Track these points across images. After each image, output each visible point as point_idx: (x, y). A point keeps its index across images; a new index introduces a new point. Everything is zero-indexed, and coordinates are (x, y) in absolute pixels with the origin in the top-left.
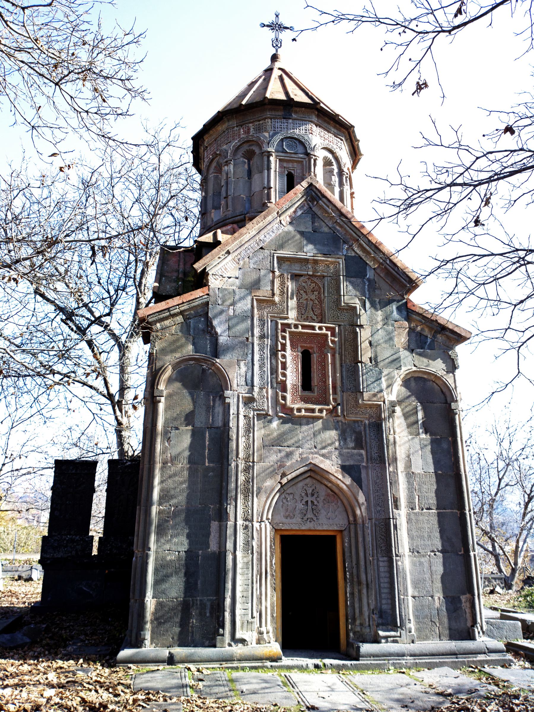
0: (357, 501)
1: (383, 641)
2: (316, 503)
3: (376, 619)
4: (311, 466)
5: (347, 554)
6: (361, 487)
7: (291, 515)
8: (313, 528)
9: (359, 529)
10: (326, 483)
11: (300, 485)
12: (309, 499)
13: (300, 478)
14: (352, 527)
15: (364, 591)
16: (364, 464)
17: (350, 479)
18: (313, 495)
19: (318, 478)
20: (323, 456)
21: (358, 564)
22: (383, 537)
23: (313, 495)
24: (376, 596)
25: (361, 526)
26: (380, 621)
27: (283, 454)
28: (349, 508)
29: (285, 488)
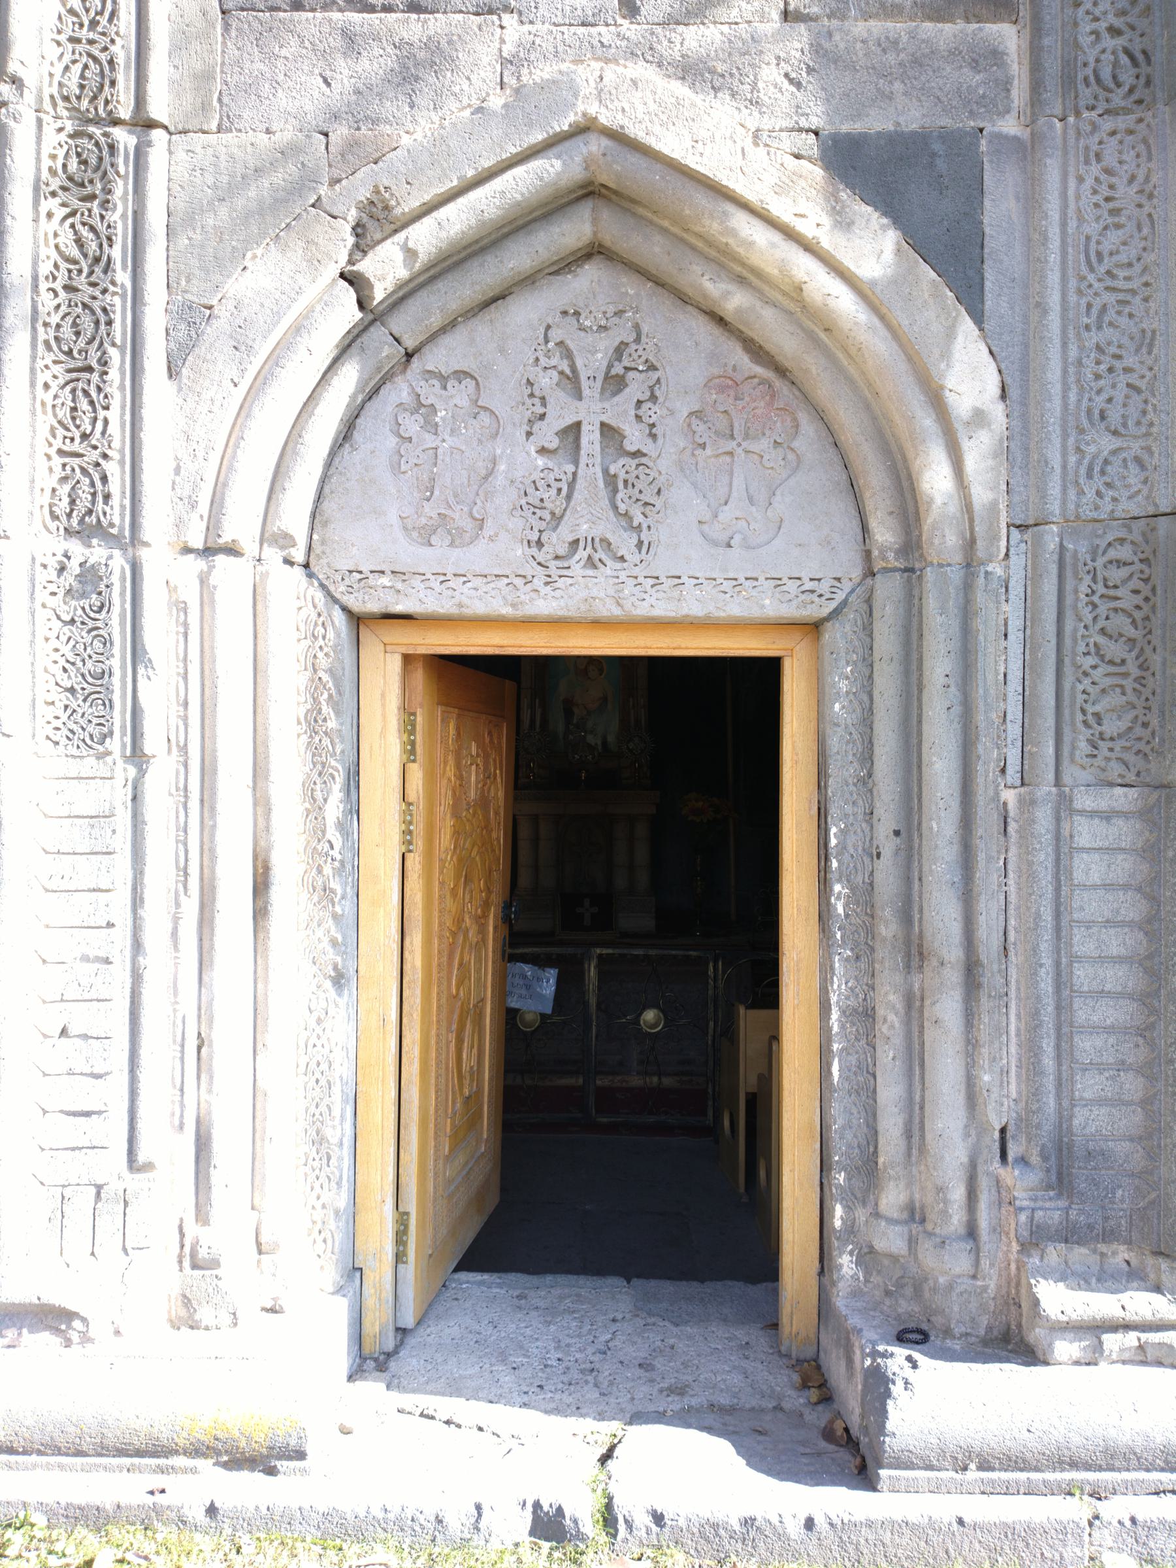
0: (936, 400)
1: (1065, 1349)
2: (634, 438)
3: (1022, 1198)
4: (595, 145)
5: (842, 772)
6: (971, 296)
7: (460, 518)
8: (607, 609)
9: (931, 604)
10: (713, 287)
11: (526, 313)
12: (591, 411)
13: (519, 257)
14: (888, 590)
15: (947, 1008)
16: (1010, 126)
17: (890, 239)
18: (614, 383)
19: (652, 249)
20: (691, 71)
21: (910, 831)
22: (1115, 650)
23: (614, 383)
24: (1031, 1048)
25: (955, 575)
26: (1052, 1213)
27: (375, 63)
28: (870, 471)
29: (408, 324)
